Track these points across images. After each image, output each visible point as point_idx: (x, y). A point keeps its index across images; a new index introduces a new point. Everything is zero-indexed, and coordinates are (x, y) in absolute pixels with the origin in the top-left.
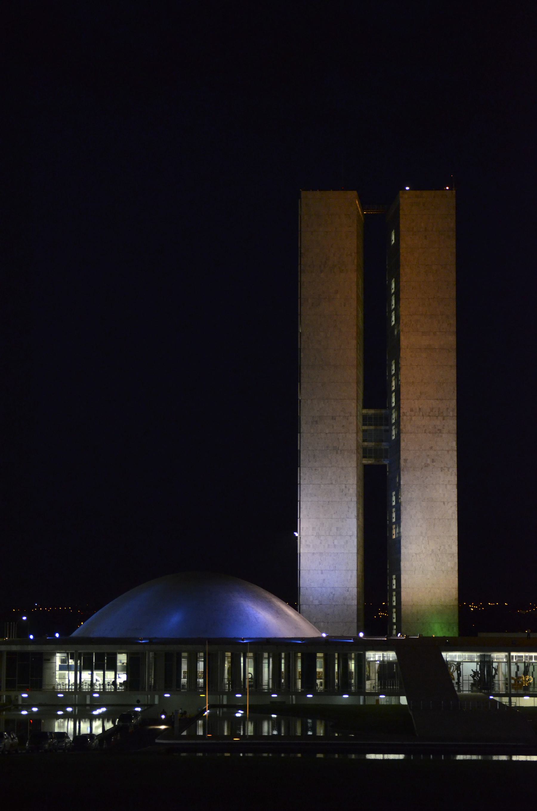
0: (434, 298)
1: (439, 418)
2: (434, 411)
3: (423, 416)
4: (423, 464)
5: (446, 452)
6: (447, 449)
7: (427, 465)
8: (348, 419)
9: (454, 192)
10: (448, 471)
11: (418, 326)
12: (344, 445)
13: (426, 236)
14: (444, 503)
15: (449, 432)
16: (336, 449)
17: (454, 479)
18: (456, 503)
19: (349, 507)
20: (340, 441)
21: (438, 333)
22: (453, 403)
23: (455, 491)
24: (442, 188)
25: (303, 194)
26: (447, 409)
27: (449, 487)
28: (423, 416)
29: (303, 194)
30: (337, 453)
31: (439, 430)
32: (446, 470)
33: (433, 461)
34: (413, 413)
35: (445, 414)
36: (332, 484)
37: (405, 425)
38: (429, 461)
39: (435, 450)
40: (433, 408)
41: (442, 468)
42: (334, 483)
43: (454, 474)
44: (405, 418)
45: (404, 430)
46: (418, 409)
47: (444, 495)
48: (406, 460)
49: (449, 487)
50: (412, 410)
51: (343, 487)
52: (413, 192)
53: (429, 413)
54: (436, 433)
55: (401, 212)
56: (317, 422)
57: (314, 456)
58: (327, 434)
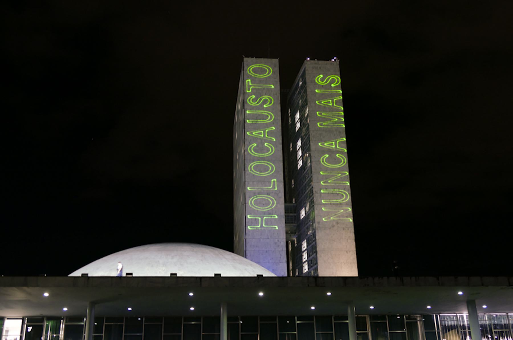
9: (338, 62)
14: (347, 252)
17: (352, 236)
18: (355, 252)
19: (281, 255)
23: (354, 243)
24: (331, 60)
25: (245, 59)
27: (349, 241)
29: (245, 59)
32: (347, 229)
33: (337, 223)
36: (268, 238)
38: (334, 223)
42: (270, 237)
44: (316, 194)
45: (316, 203)
47: (347, 246)
49: (349, 241)
51: (276, 240)
52: (312, 61)
55: (306, 72)
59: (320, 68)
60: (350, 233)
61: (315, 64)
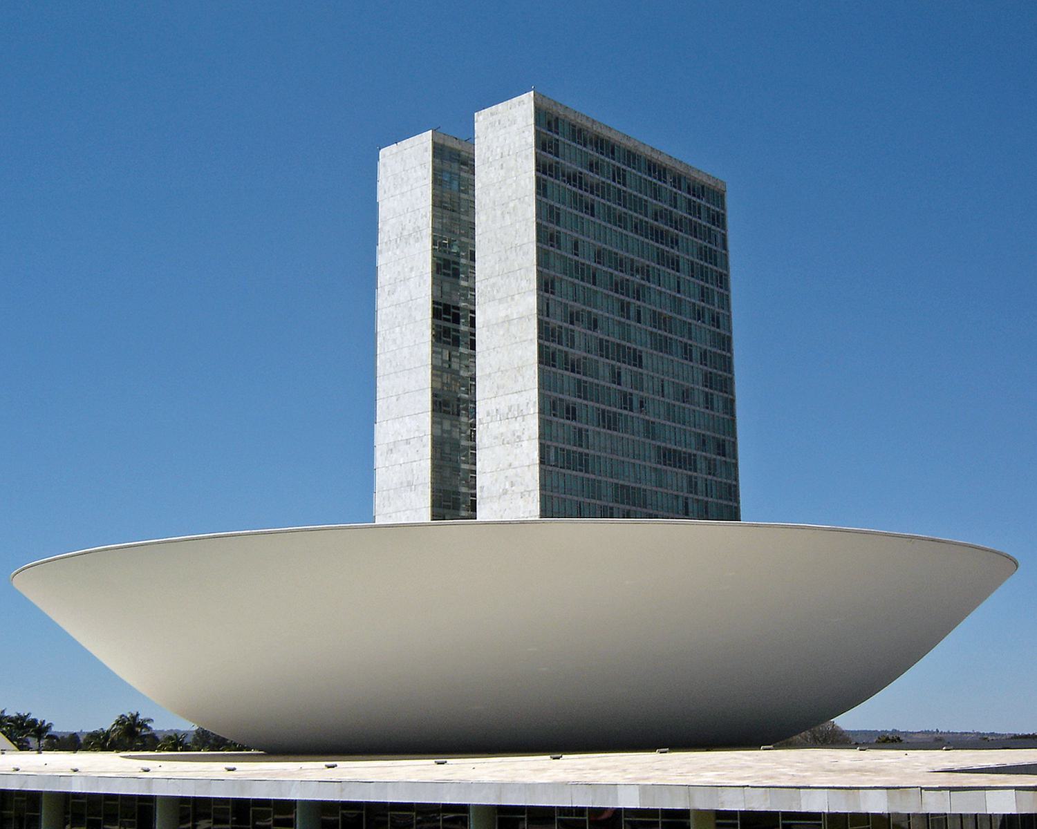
0: (511, 248)
1: (518, 418)
2: (512, 410)
3: (501, 420)
4: (501, 490)
5: (526, 468)
6: (528, 464)
7: (505, 492)
8: (422, 441)
10: (529, 496)
11: (495, 291)
12: (418, 478)
13: (502, 165)
15: (530, 439)
16: (410, 484)
20: (415, 472)
21: (517, 297)
22: (534, 395)
26: (528, 403)
28: (501, 420)
30: (411, 491)
31: (518, 437)
32: (527, 496)
33: (512, 485)
34: (489, 418)
35: (524, 414)
37: (481, 439)
39: (514, 468)
40: (511, 406)
41: (522, 493)
43: (536, 500)
45: (480, 443)
46: (495, 413)
48: (482, 488)
50: (488, 414)
53: (508, 414)
54: (515, 442)
56: (391, 450)
57: (389, 498)
58: (401, 465)
59: (499, 124)
60: (533, 503)
61: (492, 114)
